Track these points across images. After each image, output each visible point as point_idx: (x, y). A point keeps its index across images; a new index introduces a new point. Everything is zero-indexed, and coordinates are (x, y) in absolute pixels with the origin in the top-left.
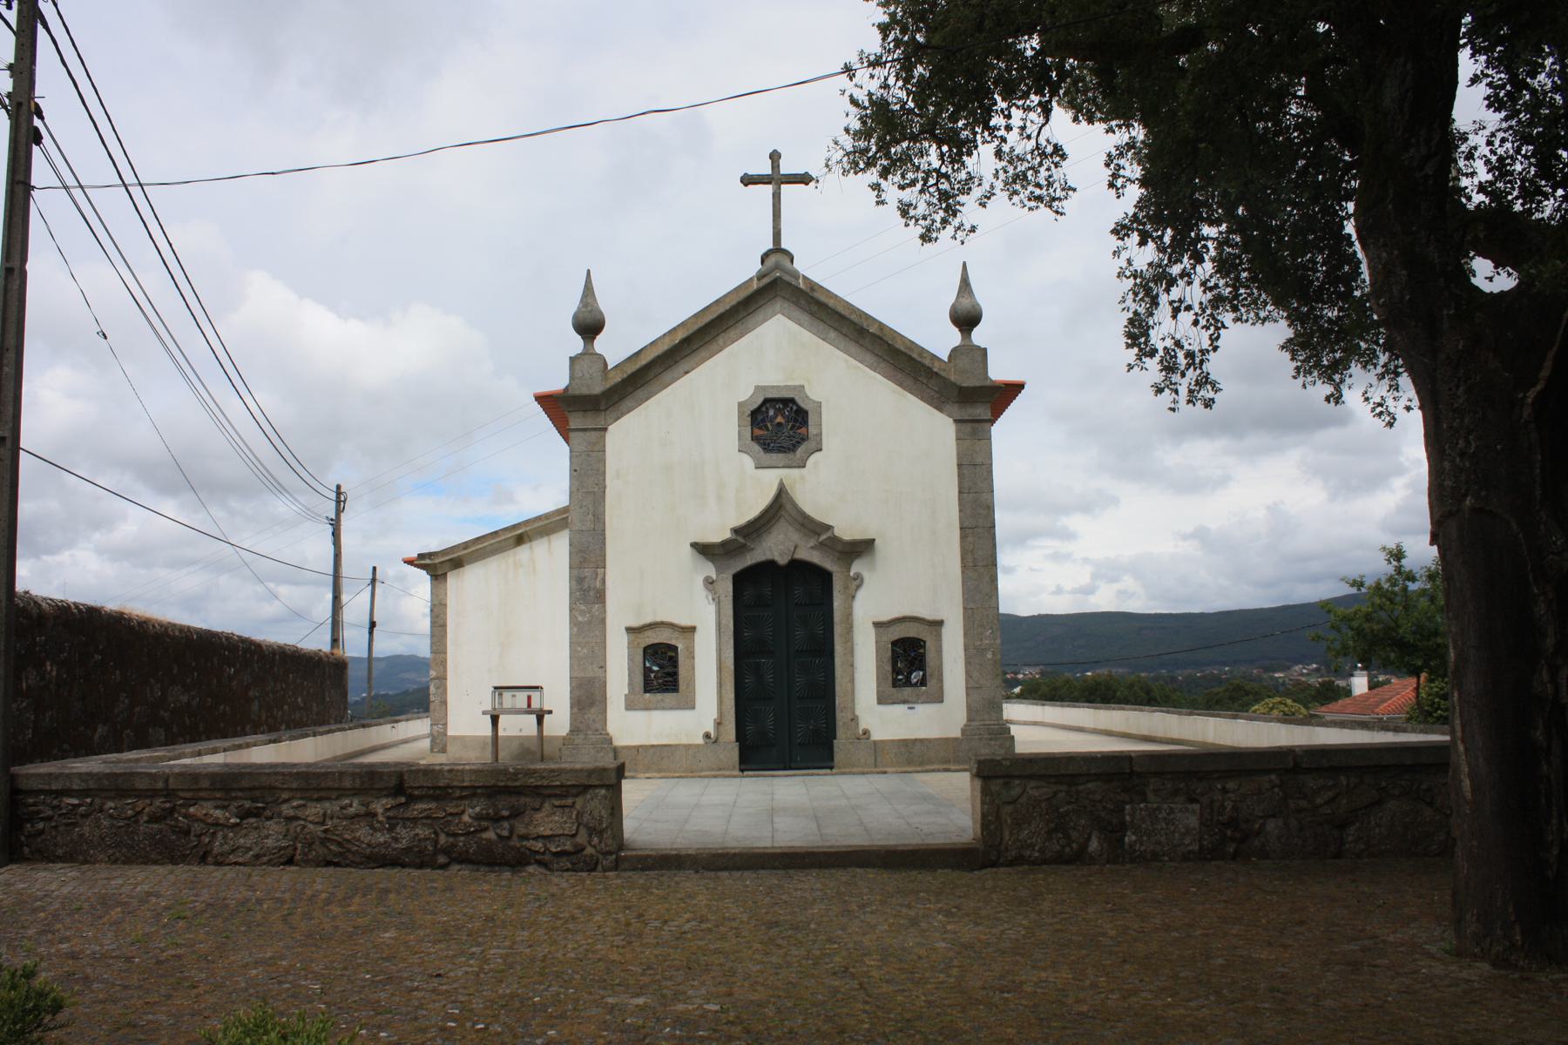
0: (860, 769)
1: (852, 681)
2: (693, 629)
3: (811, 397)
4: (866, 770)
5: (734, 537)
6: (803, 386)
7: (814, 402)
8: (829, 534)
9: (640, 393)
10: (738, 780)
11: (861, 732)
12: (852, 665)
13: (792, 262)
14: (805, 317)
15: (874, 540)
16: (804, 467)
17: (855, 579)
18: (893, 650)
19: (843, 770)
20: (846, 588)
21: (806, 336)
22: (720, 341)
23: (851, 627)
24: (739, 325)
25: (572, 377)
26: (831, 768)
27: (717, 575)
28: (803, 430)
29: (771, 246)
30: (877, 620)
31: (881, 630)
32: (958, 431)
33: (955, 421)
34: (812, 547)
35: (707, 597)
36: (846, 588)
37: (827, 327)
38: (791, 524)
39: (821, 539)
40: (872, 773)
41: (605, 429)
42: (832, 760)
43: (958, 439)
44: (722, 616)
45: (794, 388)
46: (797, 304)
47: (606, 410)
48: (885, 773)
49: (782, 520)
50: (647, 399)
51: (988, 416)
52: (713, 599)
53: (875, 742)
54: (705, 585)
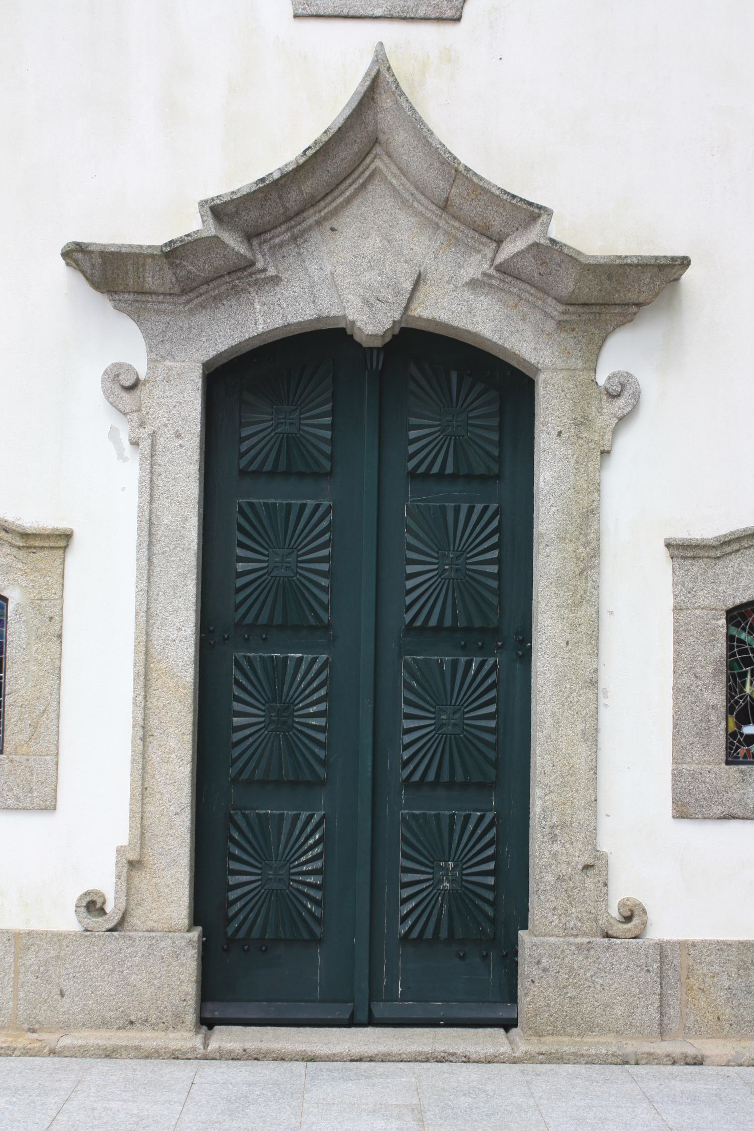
0: (607, 1044)
1: (592, 736)
2: (63, 540)
4: (632, 1046)
5: (212, 229)
8: (533, 235)
10: (182, 1071)
11: (614, 913)
12: (594, 683)
15: (684, 263)
17: (614, 396)
18: (730, 638)
19: (550, 1044)
20: (583, 422)
23: (596, 553)
26: (509, 1025)
27: (153, 362)
30: (681, 534)
31: (696, 567)
34: (473, 284)
35: (113, 434)
36: (583, 422)
38: (405, 203)
39: (502, 256)
40: (652, 1059)
42: (513, 998)
44: (162, 502)
48: (698, 1061)
49: (376, 188)
52: (135, 443)
53: (661, 947)
54: (109, 396)
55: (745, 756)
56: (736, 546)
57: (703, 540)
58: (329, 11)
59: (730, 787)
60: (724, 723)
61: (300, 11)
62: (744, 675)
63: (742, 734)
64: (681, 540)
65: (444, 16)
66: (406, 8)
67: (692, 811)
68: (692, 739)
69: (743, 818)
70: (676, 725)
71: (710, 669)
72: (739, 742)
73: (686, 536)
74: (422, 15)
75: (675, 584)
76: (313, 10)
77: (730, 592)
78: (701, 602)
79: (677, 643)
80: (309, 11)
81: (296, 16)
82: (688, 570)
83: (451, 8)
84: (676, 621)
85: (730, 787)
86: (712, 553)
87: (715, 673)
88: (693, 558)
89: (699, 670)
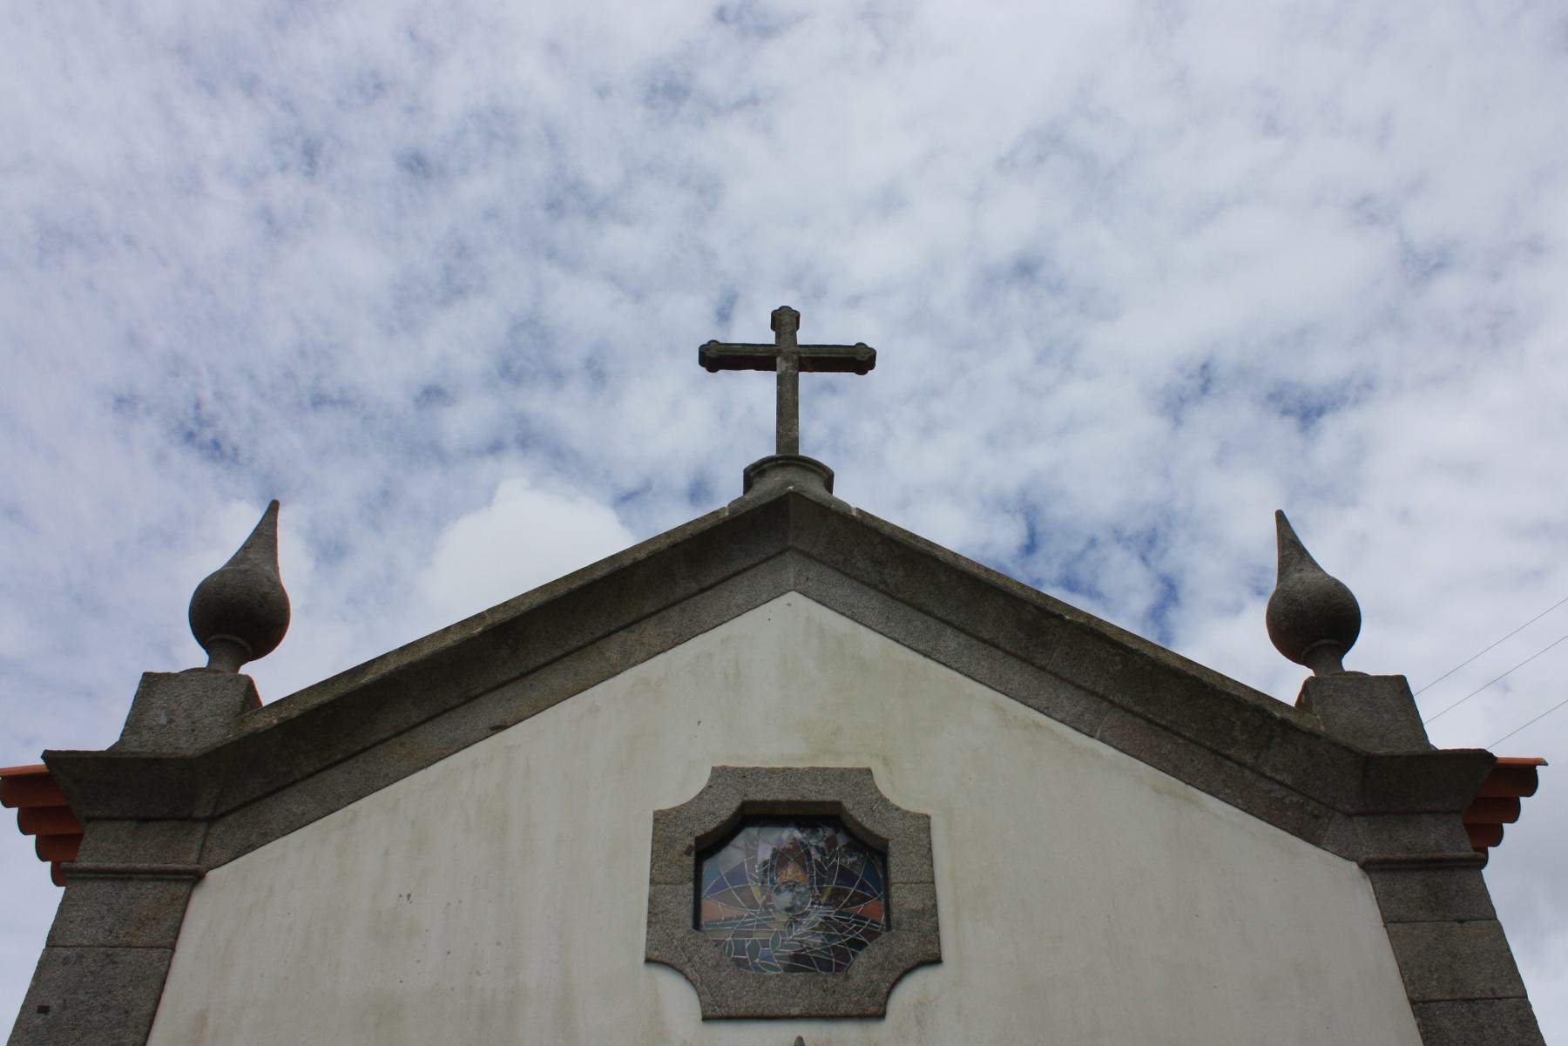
3: (895, 800)
6: (869, 771)
7: (906, 814)
9: (336, 778)
13: (829, 487)
14: (870, 601)
16: (880, 1016)
21: (871, 644)
22: (613, 649)
24: (674, 613)
25: (133, 724)
28: (872, 907)
29: (772, 451)
32: (1384, 899)
33: (1367, 867)
37: (932, 623)
41: (195, 878)
43: (1388, 921)
45: (842, 774)
46: (844, 569)
47: (212, 820)
50: (358, 797)
51: (1466, 850)
58: (742, 1012)
61: (709, 1013)
65: (867, 1013)
66: (825, 1006)
74: (843, 1012)
76: (723, 1012)
80: (719, 1012)
81: (705, 1019)
83: (873, 1005)
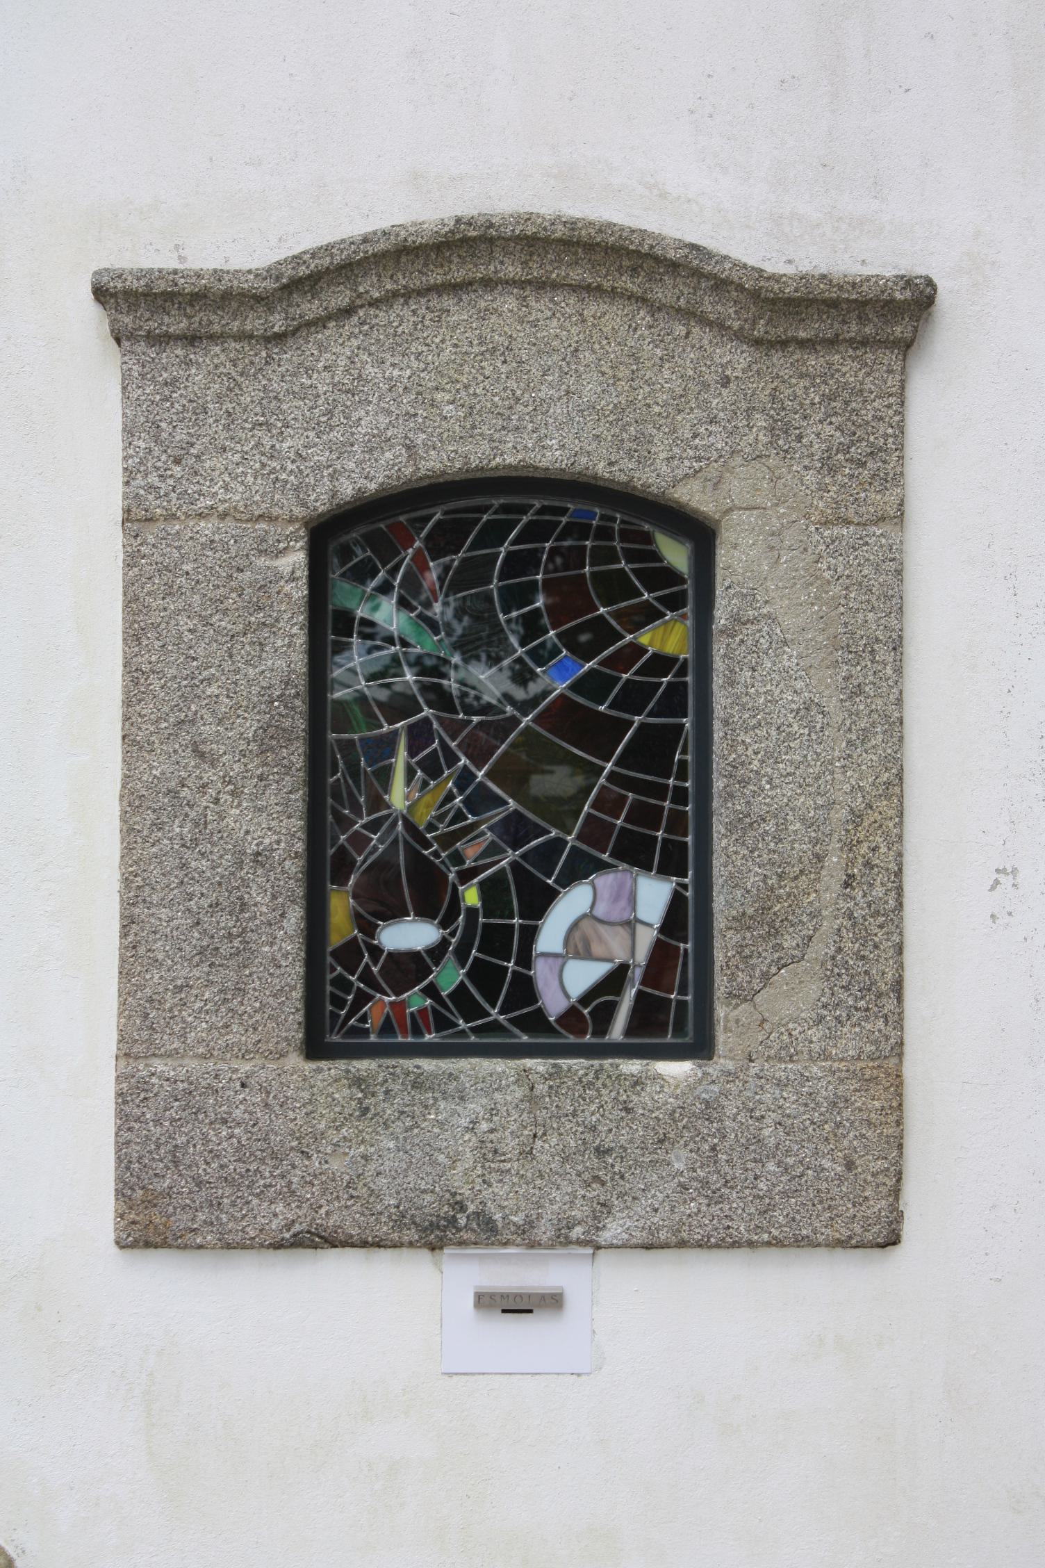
55: (387, 1028)
56: (340, 298)
57: (217, 274)
59: (318, 1136)
60: (295, 917)
62: (387, 746)
63: (376, 951)
64: (140, 274)
67: (181, 1221)
68: (183, 971)
69: (364, 1244)
70: (128, 922)
71: (250, 726)
72: (367, 977)
73: (168, 262)
75: (129, 431)
77: (319, 456)
78: (217, 493)
79: (134, 636)
82: (172, 383)
84: (131, 561)
85: (318, 1136)
86: (254, 323)
87: (267, 740)
88: (191, 339)
89: (209, 730)
